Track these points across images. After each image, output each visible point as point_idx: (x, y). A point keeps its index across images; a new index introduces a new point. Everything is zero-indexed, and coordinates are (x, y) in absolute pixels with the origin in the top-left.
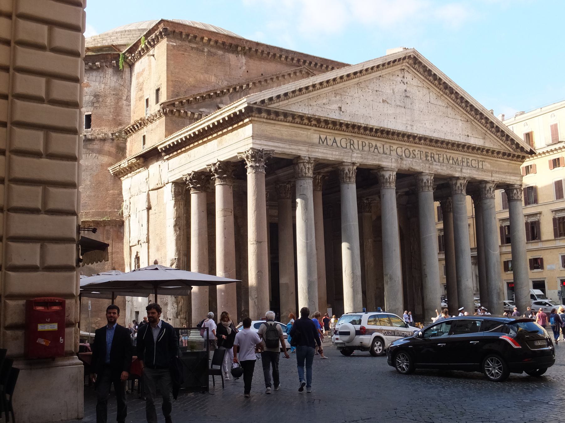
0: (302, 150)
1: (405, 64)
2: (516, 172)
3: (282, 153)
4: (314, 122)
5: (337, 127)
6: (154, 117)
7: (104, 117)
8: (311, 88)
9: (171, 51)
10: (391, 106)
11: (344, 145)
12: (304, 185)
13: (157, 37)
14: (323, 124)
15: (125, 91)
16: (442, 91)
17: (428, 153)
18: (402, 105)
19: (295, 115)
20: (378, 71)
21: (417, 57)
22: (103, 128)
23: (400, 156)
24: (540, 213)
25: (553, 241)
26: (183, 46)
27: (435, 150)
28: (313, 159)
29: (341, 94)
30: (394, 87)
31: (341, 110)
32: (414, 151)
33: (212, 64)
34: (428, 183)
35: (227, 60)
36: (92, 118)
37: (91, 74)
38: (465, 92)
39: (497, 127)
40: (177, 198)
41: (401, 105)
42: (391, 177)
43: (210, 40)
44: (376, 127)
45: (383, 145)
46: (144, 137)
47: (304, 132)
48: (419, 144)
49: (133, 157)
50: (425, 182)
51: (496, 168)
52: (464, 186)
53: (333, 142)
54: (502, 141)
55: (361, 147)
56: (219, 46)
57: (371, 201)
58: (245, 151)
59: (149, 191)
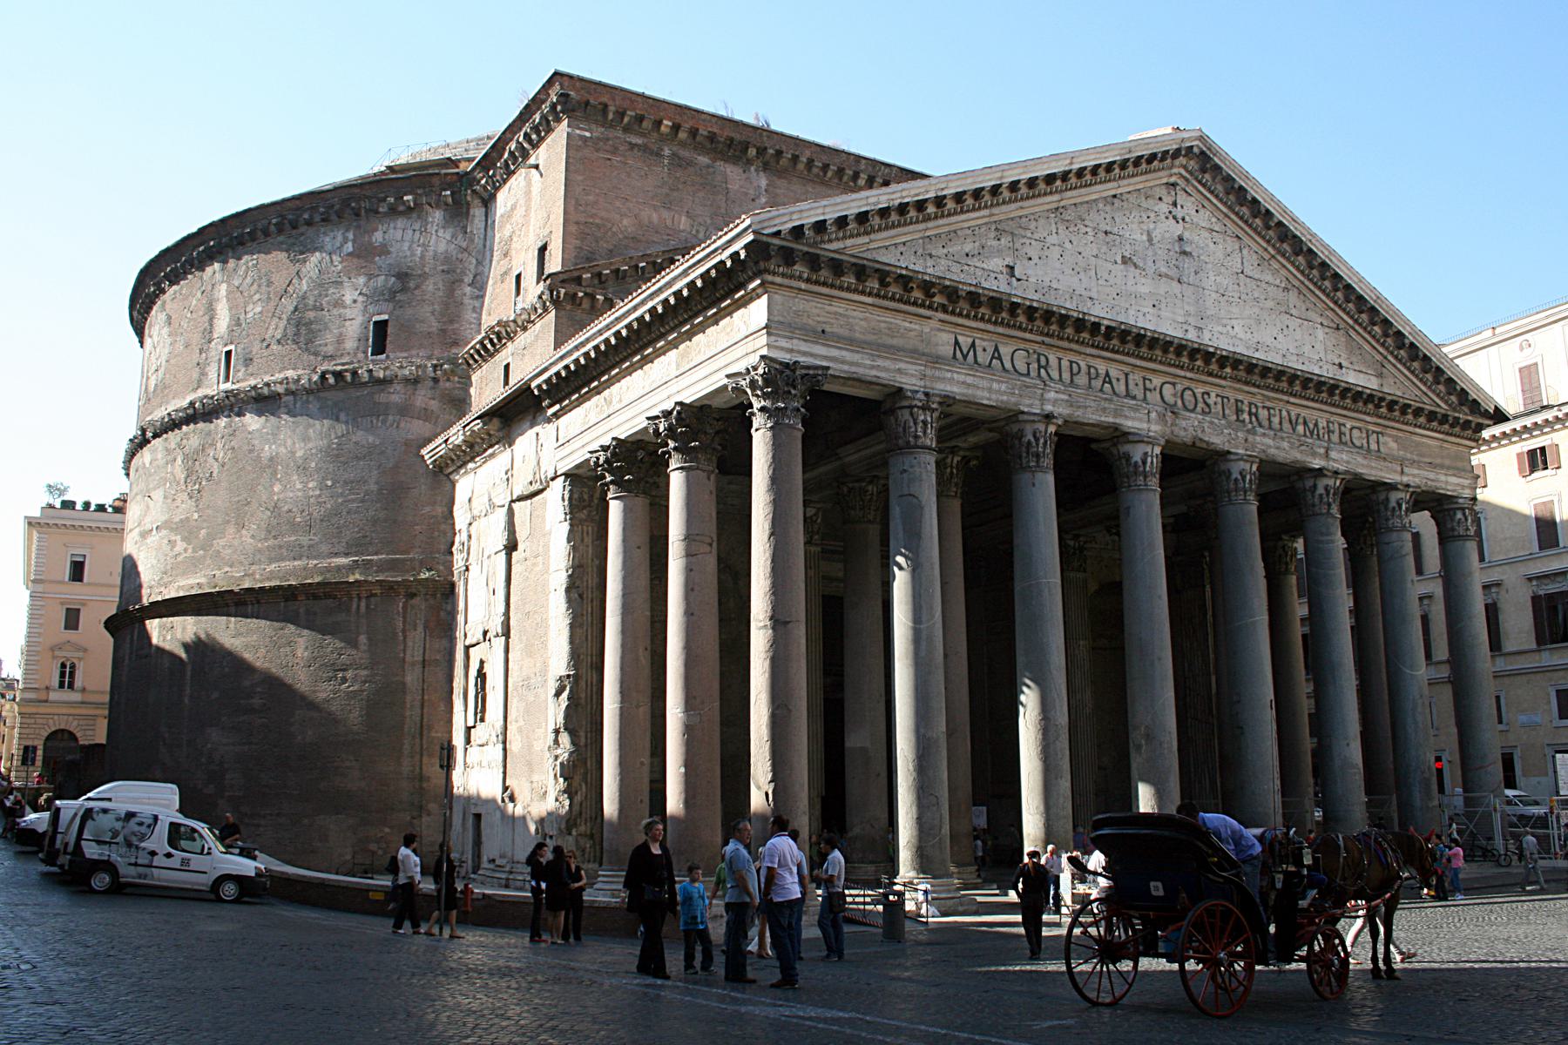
0: (906, 374)
1: (1177, 170)
2: (1459, 464)
3: (849, 379)
4: (938, 299)
5: (1004, 315)
6: (529, 314)
7: (418, 326)
8: (931, 209)
9: (577, 150)
10: (1144, 273)
12: (911, 470)
13: (544, 118)
14: (964, 306)
15: (470, 263)
16: (1273, 246)
17: (1242, 402)
18: (1173, 272)
19: (888, 273)
20: (1110, 181)
21: (1208, 152)
22: (414, 352)
23: (1171, 406)
24: (1498, 584)
25: (1533, 654)
26: (608, 139)
27: (1259, 397)
28: (938, 399)
29: (1012, 233)
30: (1152, 226)
31: (1013, 275)
32: (1206, 396)
33: (680, 186)
34: (1244, 481)
35: (719, 178)
36: (390, 330)
37: (392, 225)
38: (1332, 252)
39: (1412, 344)
40: (577, 515)
42: (1149, 459)
43: (676, 128)
44: (1106, 322)
45: (1127, 375)
46: (507, 367)
47: (913, 326)
48: (1220, 377)
49: (476, 415)
50: (1236, 480)
51: (1411, 453)
52: (1334, 495)
53: (993, 357)
54: (1425, 384)
55: (1066, 376)
56: (699, 143)
57: (1085, 543)
58: (748, 369)
59: (513, 501)
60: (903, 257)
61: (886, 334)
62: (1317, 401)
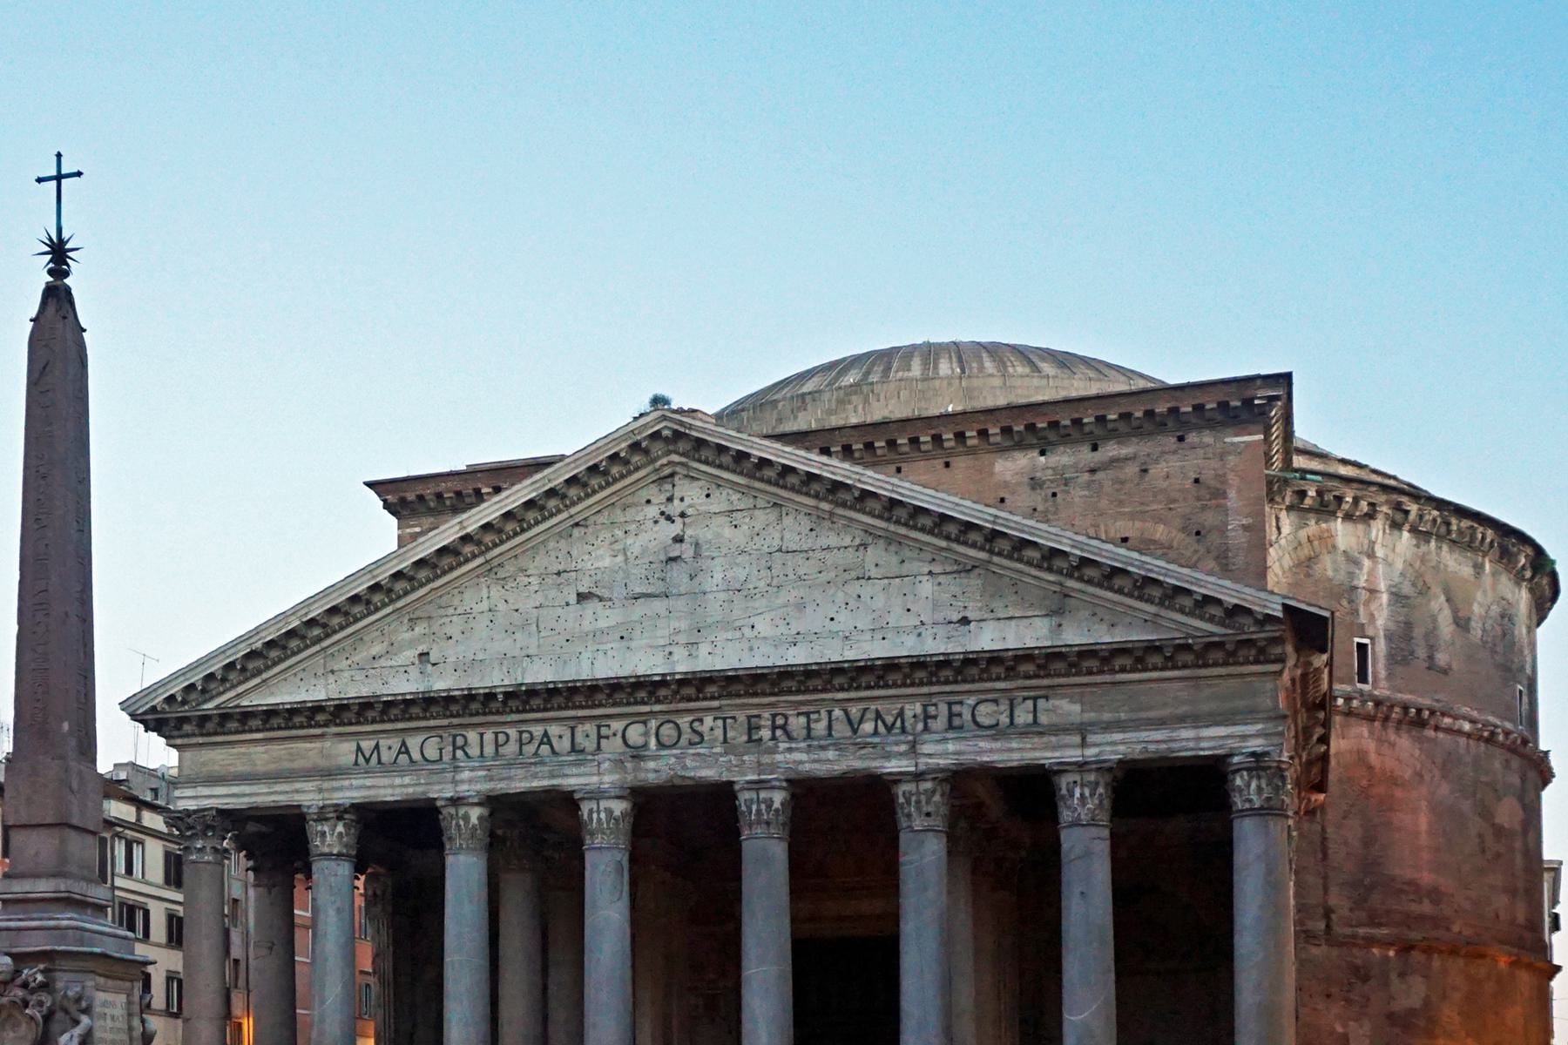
10: (610, 603)
11: (432, 753)
16: (827, 501)
17: (758, 716)
18: (657, 587)
20: (552, 515)
21: (682, 430)
28: (332, 809)
29: (429, 617)
31: (428, 661)
32: (696, 724)
34: (750, 813)
41: (649, 591)
44: (498, 690)
45: (573, 729)
47: (313, 745)
48: (705, 699)
52: (918, 802)
53: (400, 752)
55: (489, 749)
60: (303, 683)
61: (286, 760)
62: (887, 686)
